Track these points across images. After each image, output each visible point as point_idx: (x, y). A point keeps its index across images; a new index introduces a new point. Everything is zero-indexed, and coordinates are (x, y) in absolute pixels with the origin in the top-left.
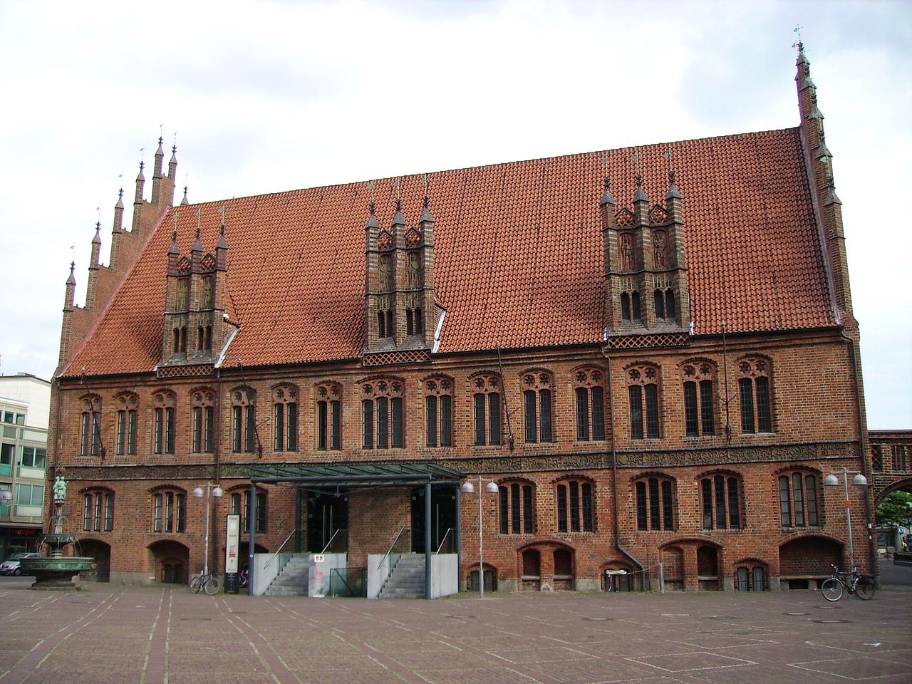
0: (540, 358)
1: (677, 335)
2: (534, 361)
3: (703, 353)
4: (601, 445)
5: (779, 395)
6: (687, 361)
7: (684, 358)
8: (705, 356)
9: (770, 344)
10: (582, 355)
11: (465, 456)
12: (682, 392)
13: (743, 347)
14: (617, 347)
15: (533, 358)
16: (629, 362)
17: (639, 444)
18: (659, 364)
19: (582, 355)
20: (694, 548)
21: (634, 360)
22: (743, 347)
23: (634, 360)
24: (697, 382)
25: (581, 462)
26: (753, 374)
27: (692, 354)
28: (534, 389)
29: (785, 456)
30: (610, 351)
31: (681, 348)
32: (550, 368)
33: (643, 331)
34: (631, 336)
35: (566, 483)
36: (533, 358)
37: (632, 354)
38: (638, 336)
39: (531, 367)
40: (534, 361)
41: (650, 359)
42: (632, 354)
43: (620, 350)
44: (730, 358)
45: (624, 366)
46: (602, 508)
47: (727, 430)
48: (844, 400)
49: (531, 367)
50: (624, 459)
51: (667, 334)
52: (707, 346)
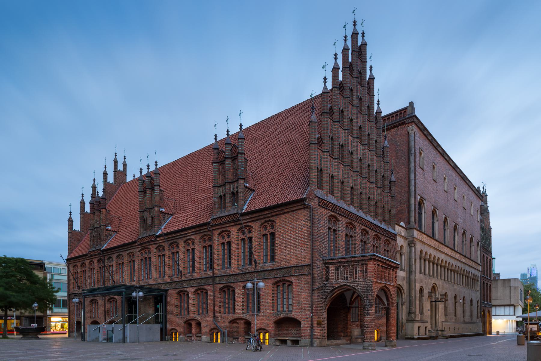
1: (235, 214)
4: (210, 273)
5: (277, 242)
6: (242, 228)
7: (239, 226)
8: (248, 224)
11: (168, 281)
12: (240, 244)
13: (262, 217)
16: (219, 231)
17: (223, 272)
20: (242, 322)
21: (221, 230)
22: (262, 217)
23: (221, 230)
24: (246, 238)
25: (203, 282)
26: (268, 231)
29: (280, 274)
30: (213, 226)
33: (225, 214)
34: (219, 218)
37: (220, 227)
38: (221, 217)
41: (227, 229)
42: (220, 227)
43: (215, 225)
44: (258, 223)
47: (255, 261)
50: (217, 279)
51: (232, 215)
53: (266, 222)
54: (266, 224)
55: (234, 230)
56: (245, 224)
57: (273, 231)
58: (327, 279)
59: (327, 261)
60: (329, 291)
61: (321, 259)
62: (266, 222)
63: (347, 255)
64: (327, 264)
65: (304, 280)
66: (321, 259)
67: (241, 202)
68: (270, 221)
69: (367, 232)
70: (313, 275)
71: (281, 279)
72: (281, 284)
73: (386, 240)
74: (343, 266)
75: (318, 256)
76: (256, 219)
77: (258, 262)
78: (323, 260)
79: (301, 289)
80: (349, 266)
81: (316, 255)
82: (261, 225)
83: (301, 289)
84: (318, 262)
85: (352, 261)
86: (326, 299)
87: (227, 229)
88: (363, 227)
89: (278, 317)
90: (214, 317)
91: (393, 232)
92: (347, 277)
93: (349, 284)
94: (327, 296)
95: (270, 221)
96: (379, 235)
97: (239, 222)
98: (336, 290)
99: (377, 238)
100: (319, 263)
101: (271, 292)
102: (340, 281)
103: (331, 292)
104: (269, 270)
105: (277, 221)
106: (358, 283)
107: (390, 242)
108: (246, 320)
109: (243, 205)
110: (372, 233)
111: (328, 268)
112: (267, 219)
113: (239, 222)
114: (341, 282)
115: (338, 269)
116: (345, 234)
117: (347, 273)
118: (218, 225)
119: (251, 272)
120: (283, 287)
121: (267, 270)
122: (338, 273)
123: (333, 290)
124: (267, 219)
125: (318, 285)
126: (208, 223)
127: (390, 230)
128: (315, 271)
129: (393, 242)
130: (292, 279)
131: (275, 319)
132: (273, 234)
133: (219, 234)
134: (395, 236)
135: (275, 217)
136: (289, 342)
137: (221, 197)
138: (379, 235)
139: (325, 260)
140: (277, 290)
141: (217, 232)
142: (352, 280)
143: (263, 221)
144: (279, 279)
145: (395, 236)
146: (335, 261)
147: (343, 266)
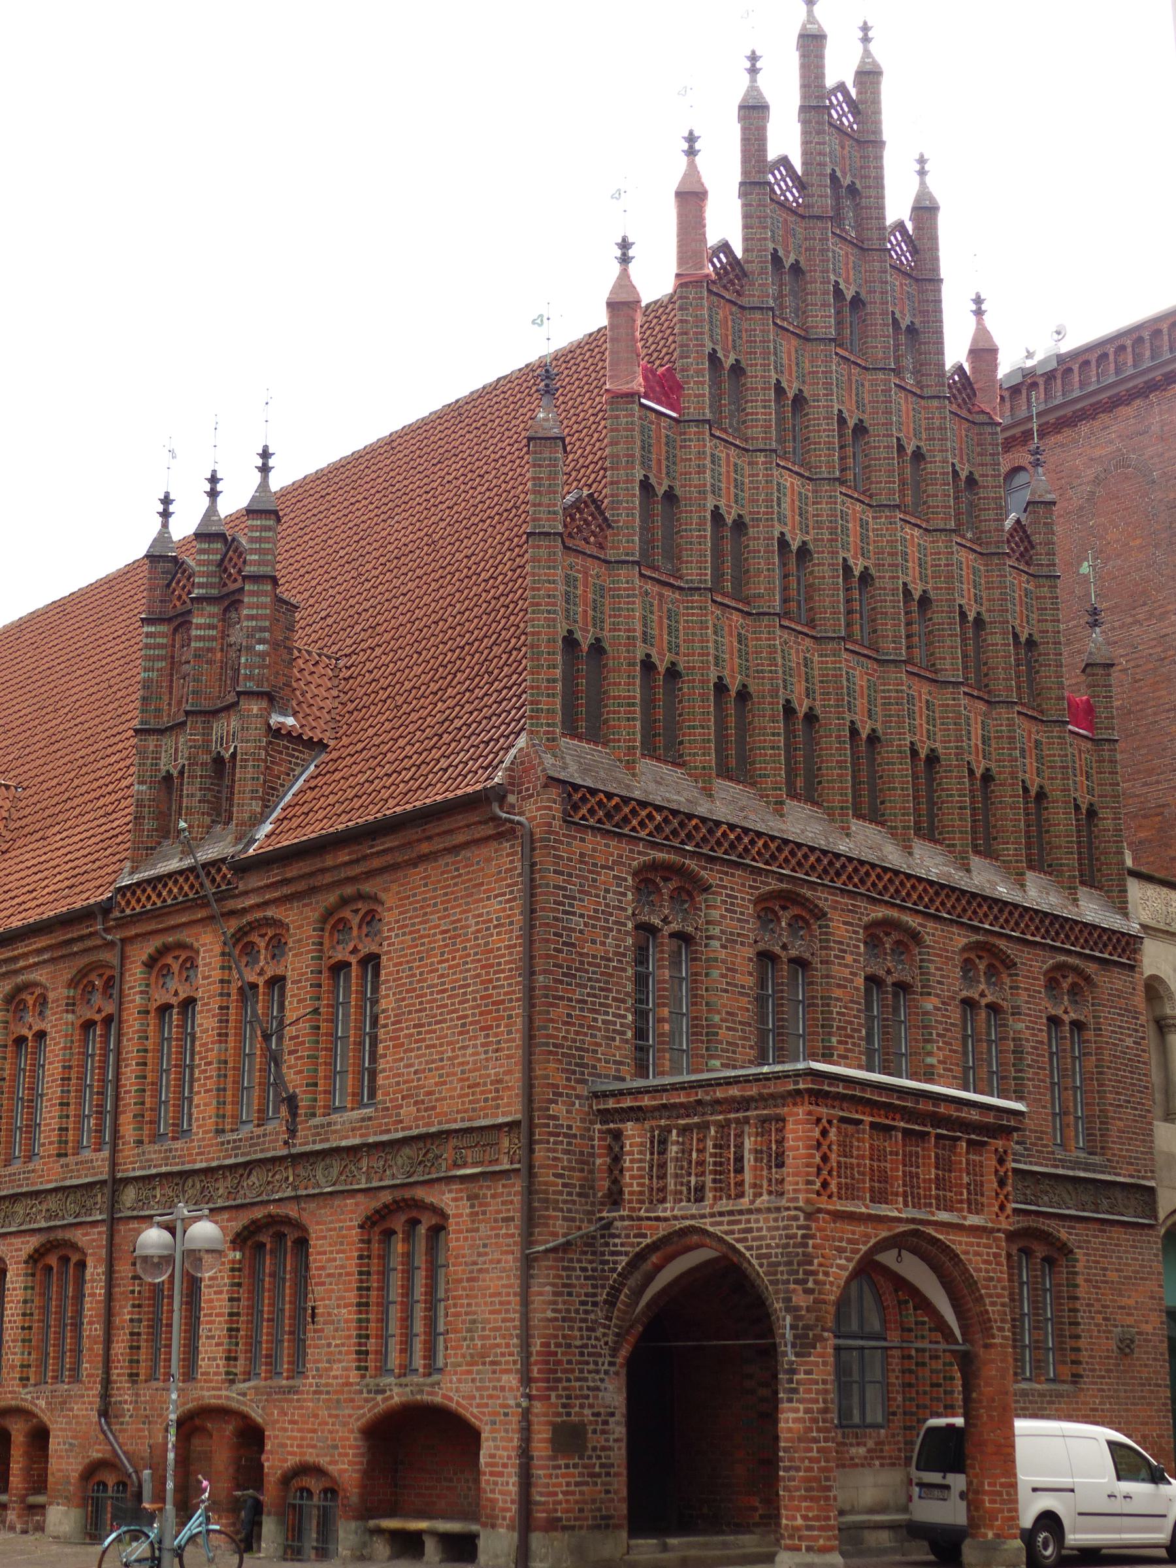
0: (25, 956)
2: (21, 963)
3: (258, 906)
7: (233, 924)
9: (376, 863)
10: (81, 938)
13: (328, 879)
14: (128, 912)
15: (15, 959)
18: (196, 945)
19: (81, 938)
22: (328, 879)
26: (355, 951)
27: (244, 911)
28: (25, 1032)
30: (123, 923)
31: (221, 897)
32: (43, 980)
35: (53, 1260)
36: (15, 959)
39: (20, 979)
40: (21, 963)
45: (144, 957)
46: (91, 1323)
48: (502, 1002)
49: (20, 979)
52: (267, 886)
53: (344, 902)
54: (347, 913)
55: (209, 946)
56: (258, 915)
57: (374, 948)
58: (615, 1198)
59: (611, 1104)
60: (624, 1260)
61: (582, 1090)
62: (344, 902)
63: (762, 1060)
64: (611, 1114)
65: (494, 1205)
66: (582, 1090)
67: (245, 805)
68: (360, 896)
69: (915, 937)
70: (531, 1175)
71: (399, 1194)
72: (398, 1223)
73: (1060, 967)
74: (685, 1130)
75: (560, 1079)
76: (301, 886)
77: (304, 1102)
78: (595, 1095)
79: (483, 1252)
80: (705, 1126)
81: (550, 1071)
82: (325, 918)
83: (483, 1252)
84: (558, 1109)
85: (717, 1102)
86: (611, 1303)
87: (184, 936)
88: (880, 913)
89: (381, 1404)
90: (105, 1396)
91: (1114, 922)
92: (700, 1189)
93: (707, 1224)
94: (615, 1291)
95: (360, 896)
96: (1002, 944)
97: (232, 904)
98: (654, 1259)
99: (988, 959)
100: (566, 1113)
101: (352, 1266)
102: (666, 1210)
103: (633, 1265)
104: (349, 1149)
105: (389, 899)
106: (757, 1223)
107: (1088, 979)
108: (245, 1417)
109: (257, 820)
110: (945, 942)
111: (617, 1135)
112: (349, 890)
113: (232, 904)
114: (676, 1212)
115: (663, 1142)
116: (750, 952)
117: (701, 1163)
118: (144, 916)
119: (274, 1160)
120: (409, 1237)
121: (337, 1150)
122: (663, 1165)
123: (641, 1256)
124: (349, 890)
125: (560, 1226)
126: (105, 909)
127: (1091, 910)
128: (540, 1152)
129: (1109, 982)
130: (447, 1199)
131: (365, 1411)
132: (371, 962)
133: (150, 964)
134: (1128, 944)
135: (379, 879)
136: (430, 1546)
137: (168, 777)
138: (1002, 944)
139: (605, 1095)
140: (384, 1257)
141: (141, 953)
142: (725, 1205)
143: (332, 898)
144: (386, 1197)
145: (1128, 944)
146: (646, 1101)
147: (685, 1130)
